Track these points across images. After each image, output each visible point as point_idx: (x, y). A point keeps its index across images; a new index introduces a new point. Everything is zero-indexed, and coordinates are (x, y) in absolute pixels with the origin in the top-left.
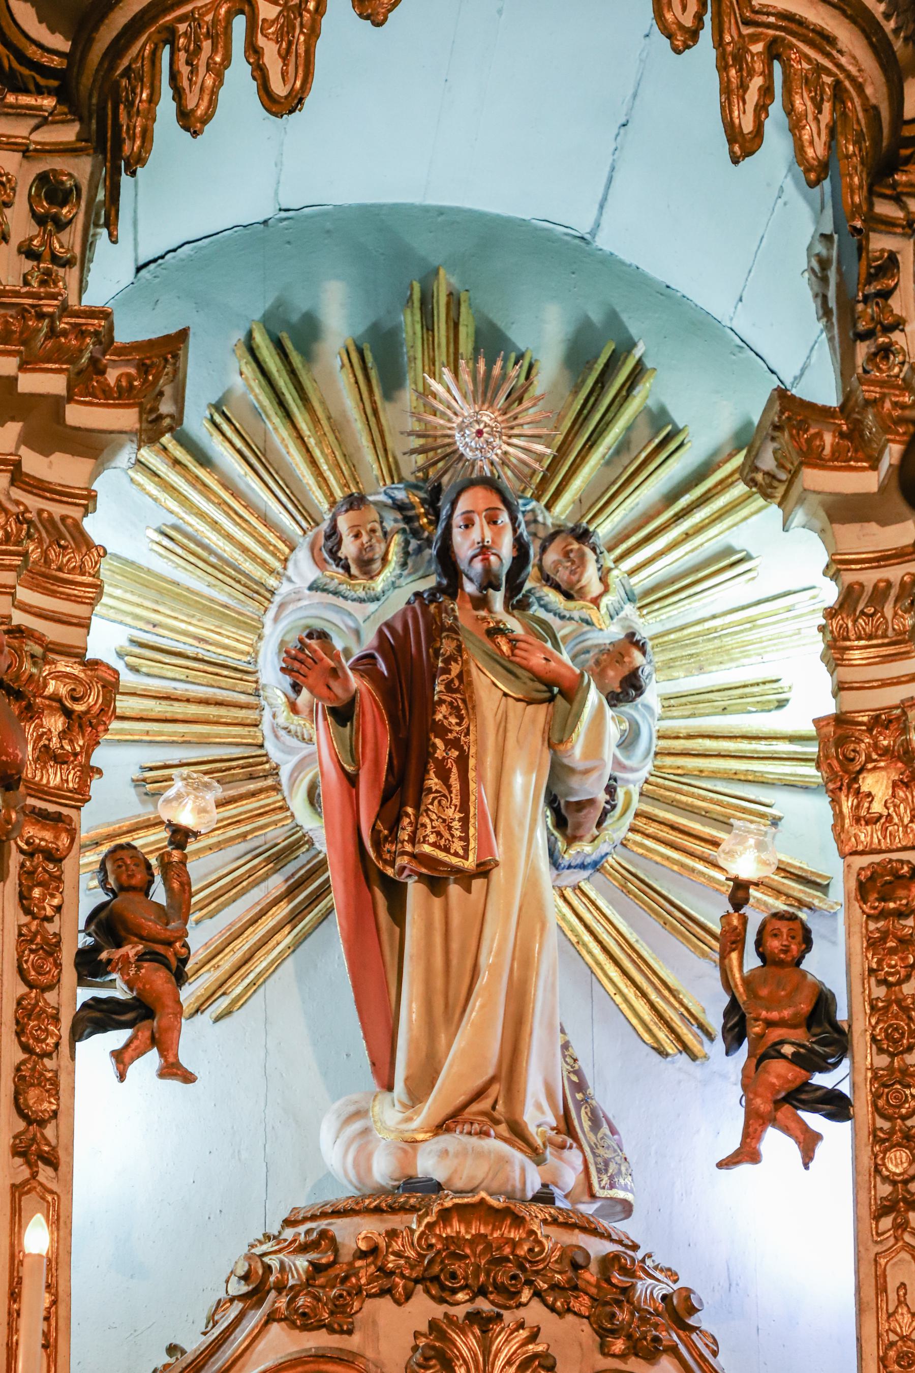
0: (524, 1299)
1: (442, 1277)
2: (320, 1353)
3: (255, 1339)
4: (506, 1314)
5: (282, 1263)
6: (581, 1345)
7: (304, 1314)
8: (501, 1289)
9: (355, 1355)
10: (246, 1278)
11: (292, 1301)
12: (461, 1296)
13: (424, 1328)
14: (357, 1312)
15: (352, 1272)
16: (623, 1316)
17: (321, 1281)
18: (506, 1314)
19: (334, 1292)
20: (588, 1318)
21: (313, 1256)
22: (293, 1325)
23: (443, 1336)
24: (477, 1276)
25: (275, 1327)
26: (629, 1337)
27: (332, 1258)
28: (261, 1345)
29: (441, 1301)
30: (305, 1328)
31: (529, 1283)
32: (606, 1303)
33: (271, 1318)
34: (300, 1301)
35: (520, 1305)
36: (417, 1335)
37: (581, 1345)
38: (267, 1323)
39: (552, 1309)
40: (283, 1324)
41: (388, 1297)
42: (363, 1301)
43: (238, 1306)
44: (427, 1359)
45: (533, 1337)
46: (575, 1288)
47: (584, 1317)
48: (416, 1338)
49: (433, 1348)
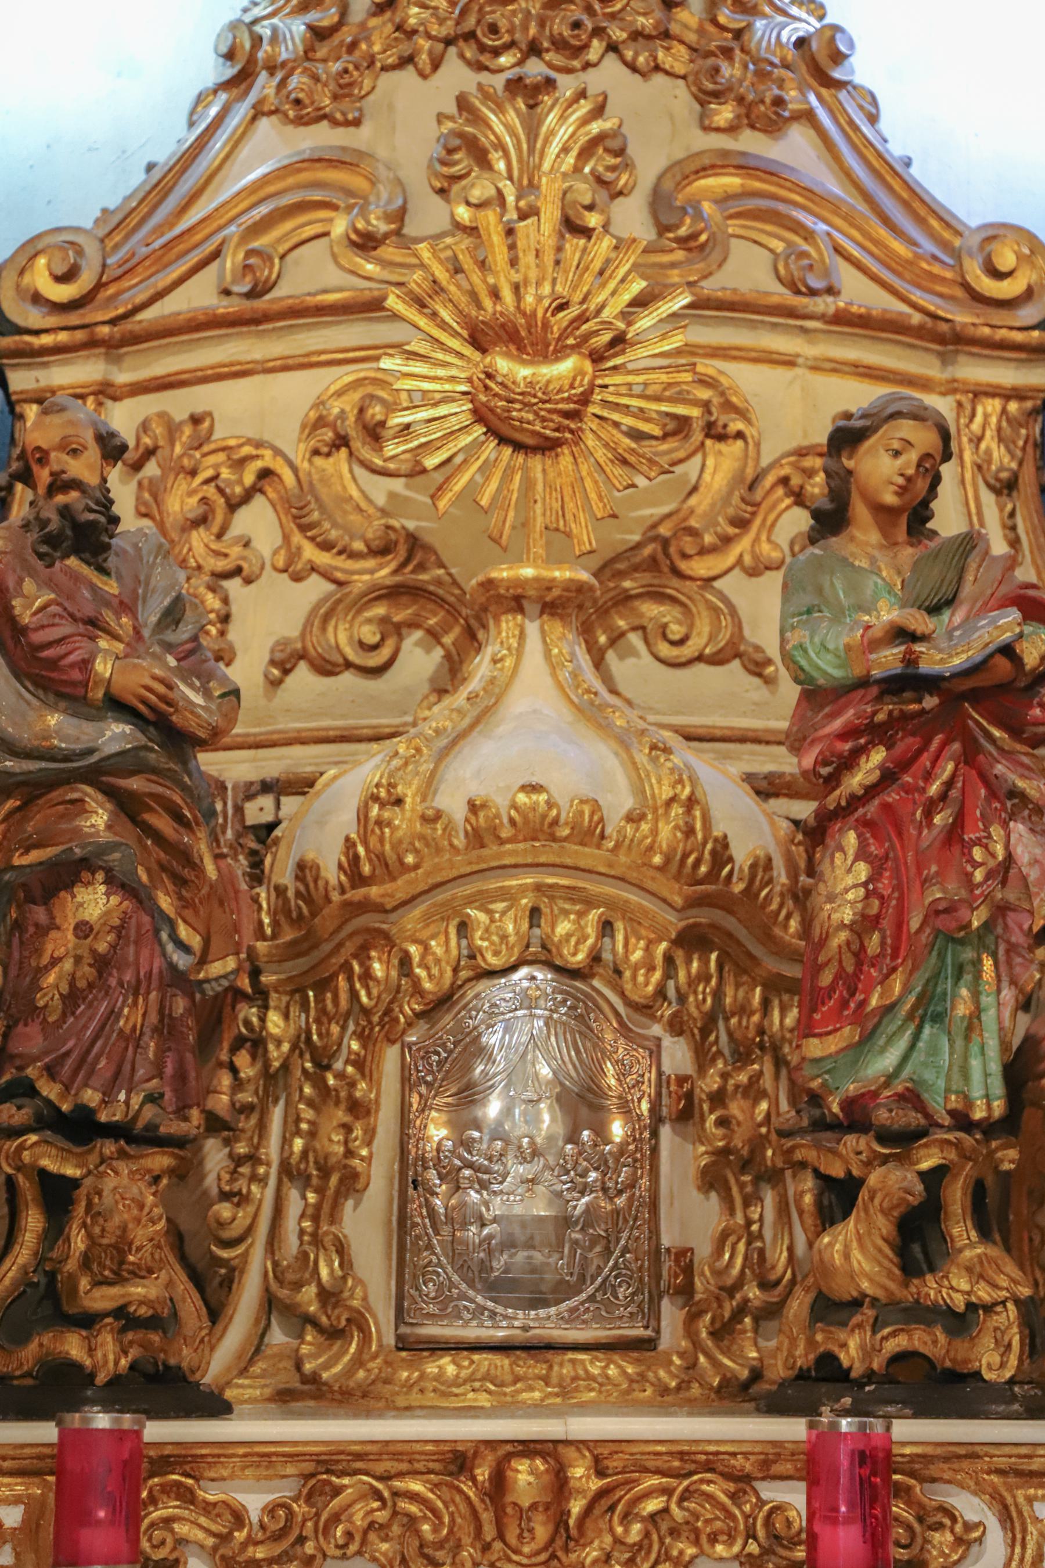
0: (593, 55)
1: (479, 33)
2: (316, 156)
3: (237, 142)
4: (561, 79)
5: (275, 30)
6: (671, 117)
7: (298, 102)
8: (560, 44)
9: (360, 153)
10: (230, 56)
11: (283, 83)
12: (504, 60)
13: (452, 109)
14: (368, 94)
15: (364, 32)
16: (727, 71)
17: (322, 52)
18: (561, 79)
19: (336, 67)
20: (684, 77)
21: (313, 16)
22: (288, 120)
23: (477, 118)
24: (525, 28)
25: (264, 123)
26: (741, 100)
27: (336, 19)
28: (245, 152)
29: (481, 67)
30: (301, 121)
31: (598, 32)
32: (709, 54)
33: (258, 112)
34: (294, 82)
35: (587, 65)
36: (441, 118)
37: (671, 117)
38: (254, 119)
39: (633, 67)
40: (274, 118)
41: (411, 68)
42: (377, 77)
43: (223, 97)
44: (450, 151)
45: (599, 111)
46: (666, 35)
47: (678, 77)
48: (439, 122)
49: (461, 135)
